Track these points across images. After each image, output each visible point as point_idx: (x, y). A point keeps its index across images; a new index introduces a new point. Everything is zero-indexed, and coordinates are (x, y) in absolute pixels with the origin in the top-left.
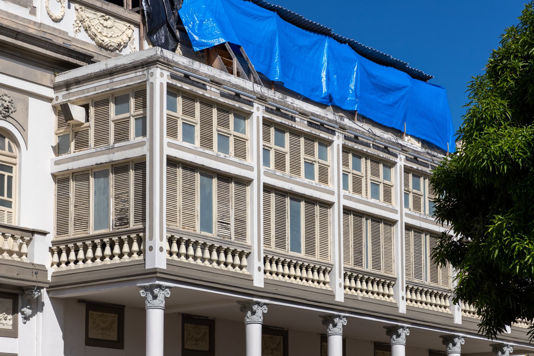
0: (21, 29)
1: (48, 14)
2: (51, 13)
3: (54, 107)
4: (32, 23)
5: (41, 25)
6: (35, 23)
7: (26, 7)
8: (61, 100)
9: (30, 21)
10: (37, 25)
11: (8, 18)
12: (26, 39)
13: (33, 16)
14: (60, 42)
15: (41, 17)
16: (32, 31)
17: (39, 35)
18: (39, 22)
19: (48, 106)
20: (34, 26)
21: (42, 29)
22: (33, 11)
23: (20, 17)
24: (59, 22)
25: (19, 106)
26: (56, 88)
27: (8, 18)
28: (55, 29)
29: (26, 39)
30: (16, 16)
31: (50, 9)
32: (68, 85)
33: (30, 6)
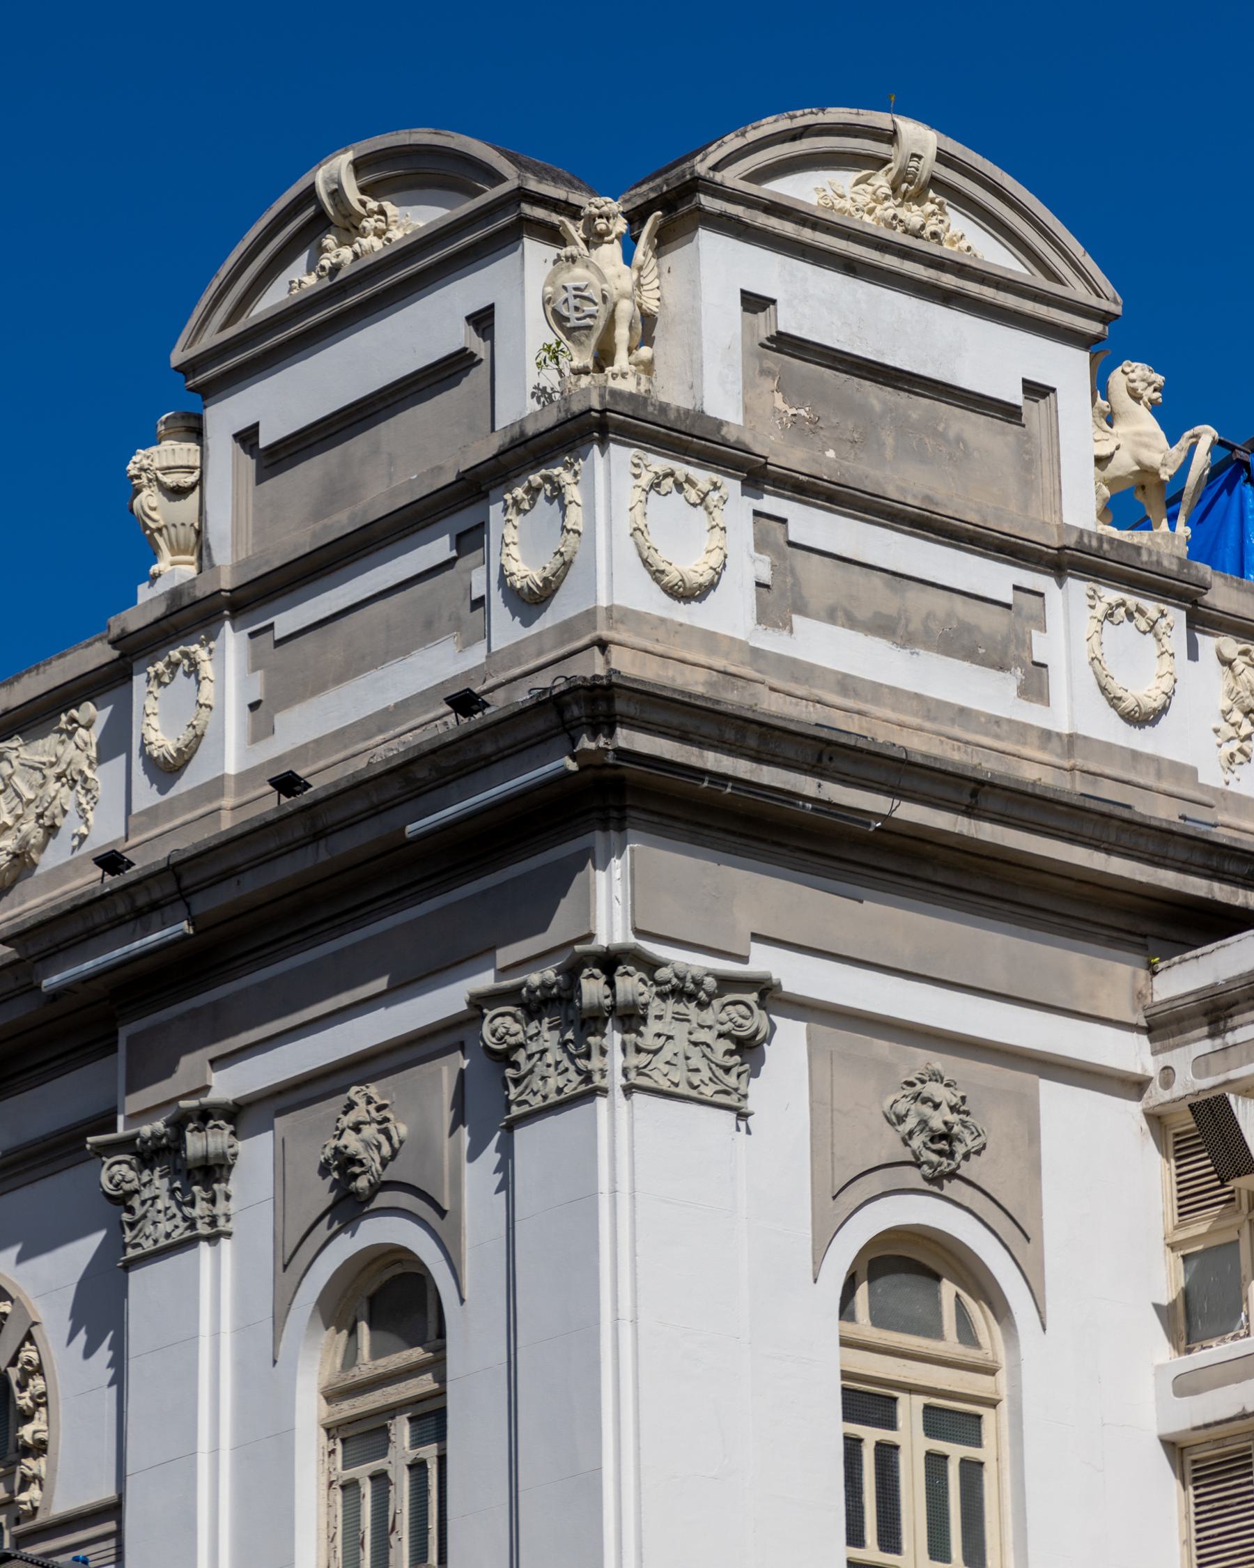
0: (990, 766)
1: (1104, 690)
2: (1115, 687)
3: (1156, 1120)
4: (1033, 738)
5: (1072, 742)
6: (1047, 736)
7: (1002, 668)
8: (1188, 1083)
9: (1021, 730)
10: (1055, 744)
11: (927, 725)
12: (1016, 812)
13: (1037, 707)
14: (1163, 812)
15: (1073, 709)
16: (1035, 771)
17: (1068, 787)
18: (1065, 729)
19: (1131, 1113)
20: (1043, 748)
21: (1080, 762)
22: (1035, 683)
23: (978, 714)
24: (1153, 723)
25: (995, 1123)
26: (1162, 1027)
27: (927, 725)
28: (1135, 756)
29: (1016, 812)
30: (963, 711)
31: (1110, 666)
32: (1216, 1011)
33: (1022, 664)
